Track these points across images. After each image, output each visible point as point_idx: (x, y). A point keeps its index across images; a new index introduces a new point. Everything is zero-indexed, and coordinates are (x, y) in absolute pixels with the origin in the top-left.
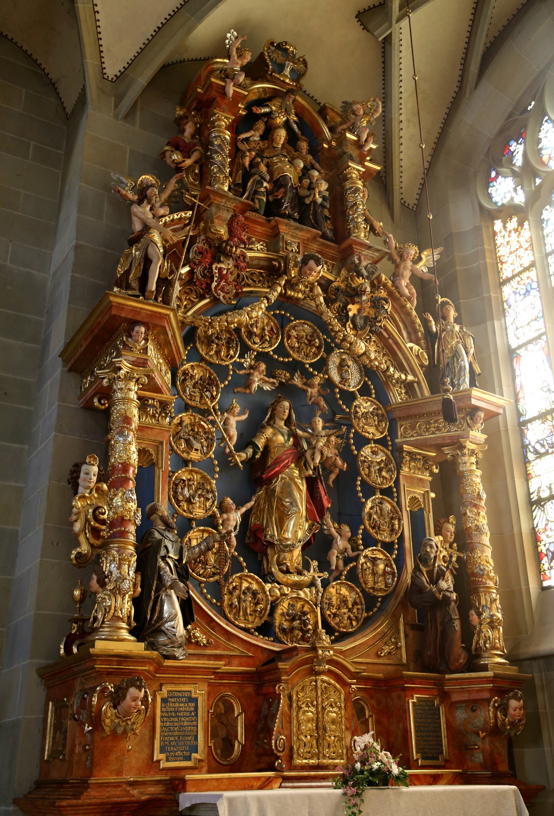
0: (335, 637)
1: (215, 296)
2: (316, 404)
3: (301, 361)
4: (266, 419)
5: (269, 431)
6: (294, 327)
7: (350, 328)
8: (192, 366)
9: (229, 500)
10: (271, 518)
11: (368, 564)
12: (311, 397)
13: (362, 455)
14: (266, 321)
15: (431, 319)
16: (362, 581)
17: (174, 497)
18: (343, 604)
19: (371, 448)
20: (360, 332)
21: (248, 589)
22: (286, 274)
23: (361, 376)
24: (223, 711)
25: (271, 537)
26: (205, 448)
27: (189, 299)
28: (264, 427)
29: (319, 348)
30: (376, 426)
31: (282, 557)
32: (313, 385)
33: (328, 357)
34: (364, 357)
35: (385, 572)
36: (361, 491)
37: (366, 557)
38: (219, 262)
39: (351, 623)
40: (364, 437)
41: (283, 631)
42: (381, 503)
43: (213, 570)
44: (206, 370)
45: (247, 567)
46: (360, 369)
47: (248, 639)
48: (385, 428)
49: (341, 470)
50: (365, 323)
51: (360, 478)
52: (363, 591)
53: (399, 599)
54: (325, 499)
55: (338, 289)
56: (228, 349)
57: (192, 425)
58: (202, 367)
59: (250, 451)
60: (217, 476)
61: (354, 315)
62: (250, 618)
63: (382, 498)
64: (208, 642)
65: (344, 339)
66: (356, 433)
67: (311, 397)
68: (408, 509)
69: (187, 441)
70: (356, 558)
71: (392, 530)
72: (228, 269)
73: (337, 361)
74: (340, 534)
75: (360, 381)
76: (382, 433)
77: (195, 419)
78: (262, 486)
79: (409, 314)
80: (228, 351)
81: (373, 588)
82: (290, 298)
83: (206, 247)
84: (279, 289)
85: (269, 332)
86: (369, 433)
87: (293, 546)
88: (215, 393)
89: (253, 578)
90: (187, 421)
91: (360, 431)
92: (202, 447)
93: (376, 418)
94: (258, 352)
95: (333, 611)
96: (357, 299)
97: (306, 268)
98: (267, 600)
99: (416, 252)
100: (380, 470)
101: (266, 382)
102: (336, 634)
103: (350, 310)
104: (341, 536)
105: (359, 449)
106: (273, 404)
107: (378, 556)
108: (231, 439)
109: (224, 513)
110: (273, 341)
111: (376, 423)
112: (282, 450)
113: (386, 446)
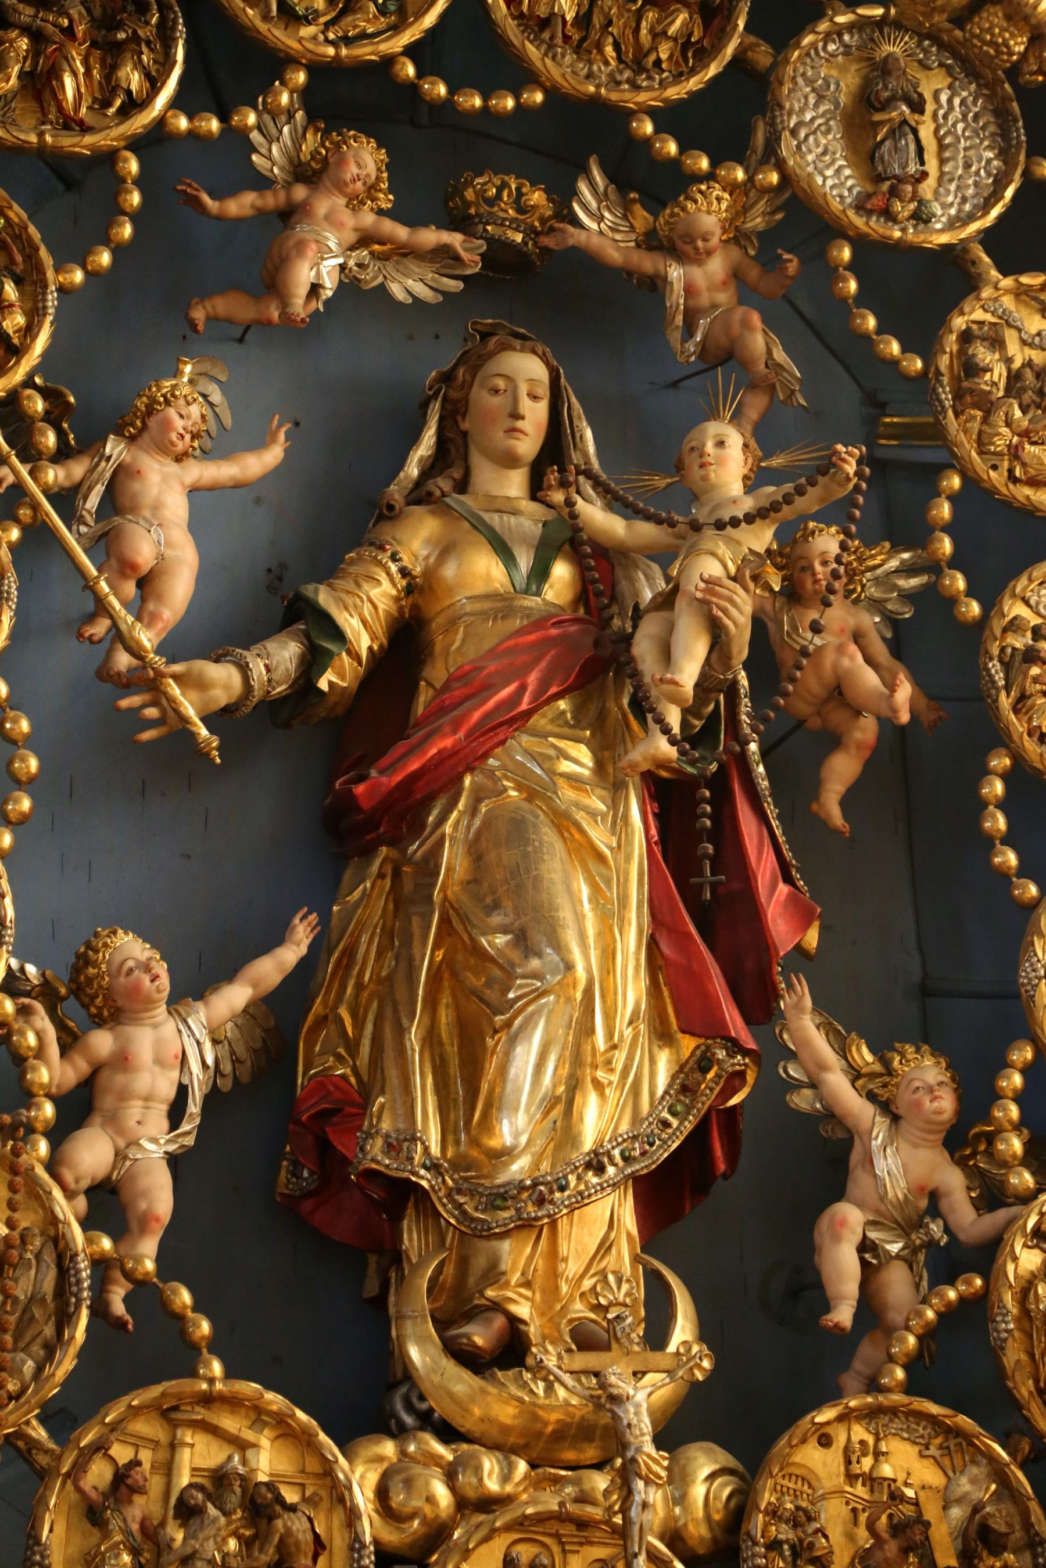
3: (595, 101)
4: (413, 470)
10: (401, 1032)
12: (691, 317)
13: (1014, 625)
23: (1005, 154)
25: (391, 1147)
28: (388, 514)
31: (479, 1263)
32: (690, 238)
33: (779, 62)
36: (1009, 840)
45: (216, 1346)
46: (1001, 114)
49: (887, 724)
51: (1001, 762)
60: (26, 804)
67: (691, 317)
74: (886, 1107)
78: (368, 852)
80: (110, 71)
89: (259, 1415)
91: (997, 478)
94: (317, 69)
98: (356, 1544)
101: (405, 252)
104: (896, 1119)
106: (447, 378)
109: (99, 1022)
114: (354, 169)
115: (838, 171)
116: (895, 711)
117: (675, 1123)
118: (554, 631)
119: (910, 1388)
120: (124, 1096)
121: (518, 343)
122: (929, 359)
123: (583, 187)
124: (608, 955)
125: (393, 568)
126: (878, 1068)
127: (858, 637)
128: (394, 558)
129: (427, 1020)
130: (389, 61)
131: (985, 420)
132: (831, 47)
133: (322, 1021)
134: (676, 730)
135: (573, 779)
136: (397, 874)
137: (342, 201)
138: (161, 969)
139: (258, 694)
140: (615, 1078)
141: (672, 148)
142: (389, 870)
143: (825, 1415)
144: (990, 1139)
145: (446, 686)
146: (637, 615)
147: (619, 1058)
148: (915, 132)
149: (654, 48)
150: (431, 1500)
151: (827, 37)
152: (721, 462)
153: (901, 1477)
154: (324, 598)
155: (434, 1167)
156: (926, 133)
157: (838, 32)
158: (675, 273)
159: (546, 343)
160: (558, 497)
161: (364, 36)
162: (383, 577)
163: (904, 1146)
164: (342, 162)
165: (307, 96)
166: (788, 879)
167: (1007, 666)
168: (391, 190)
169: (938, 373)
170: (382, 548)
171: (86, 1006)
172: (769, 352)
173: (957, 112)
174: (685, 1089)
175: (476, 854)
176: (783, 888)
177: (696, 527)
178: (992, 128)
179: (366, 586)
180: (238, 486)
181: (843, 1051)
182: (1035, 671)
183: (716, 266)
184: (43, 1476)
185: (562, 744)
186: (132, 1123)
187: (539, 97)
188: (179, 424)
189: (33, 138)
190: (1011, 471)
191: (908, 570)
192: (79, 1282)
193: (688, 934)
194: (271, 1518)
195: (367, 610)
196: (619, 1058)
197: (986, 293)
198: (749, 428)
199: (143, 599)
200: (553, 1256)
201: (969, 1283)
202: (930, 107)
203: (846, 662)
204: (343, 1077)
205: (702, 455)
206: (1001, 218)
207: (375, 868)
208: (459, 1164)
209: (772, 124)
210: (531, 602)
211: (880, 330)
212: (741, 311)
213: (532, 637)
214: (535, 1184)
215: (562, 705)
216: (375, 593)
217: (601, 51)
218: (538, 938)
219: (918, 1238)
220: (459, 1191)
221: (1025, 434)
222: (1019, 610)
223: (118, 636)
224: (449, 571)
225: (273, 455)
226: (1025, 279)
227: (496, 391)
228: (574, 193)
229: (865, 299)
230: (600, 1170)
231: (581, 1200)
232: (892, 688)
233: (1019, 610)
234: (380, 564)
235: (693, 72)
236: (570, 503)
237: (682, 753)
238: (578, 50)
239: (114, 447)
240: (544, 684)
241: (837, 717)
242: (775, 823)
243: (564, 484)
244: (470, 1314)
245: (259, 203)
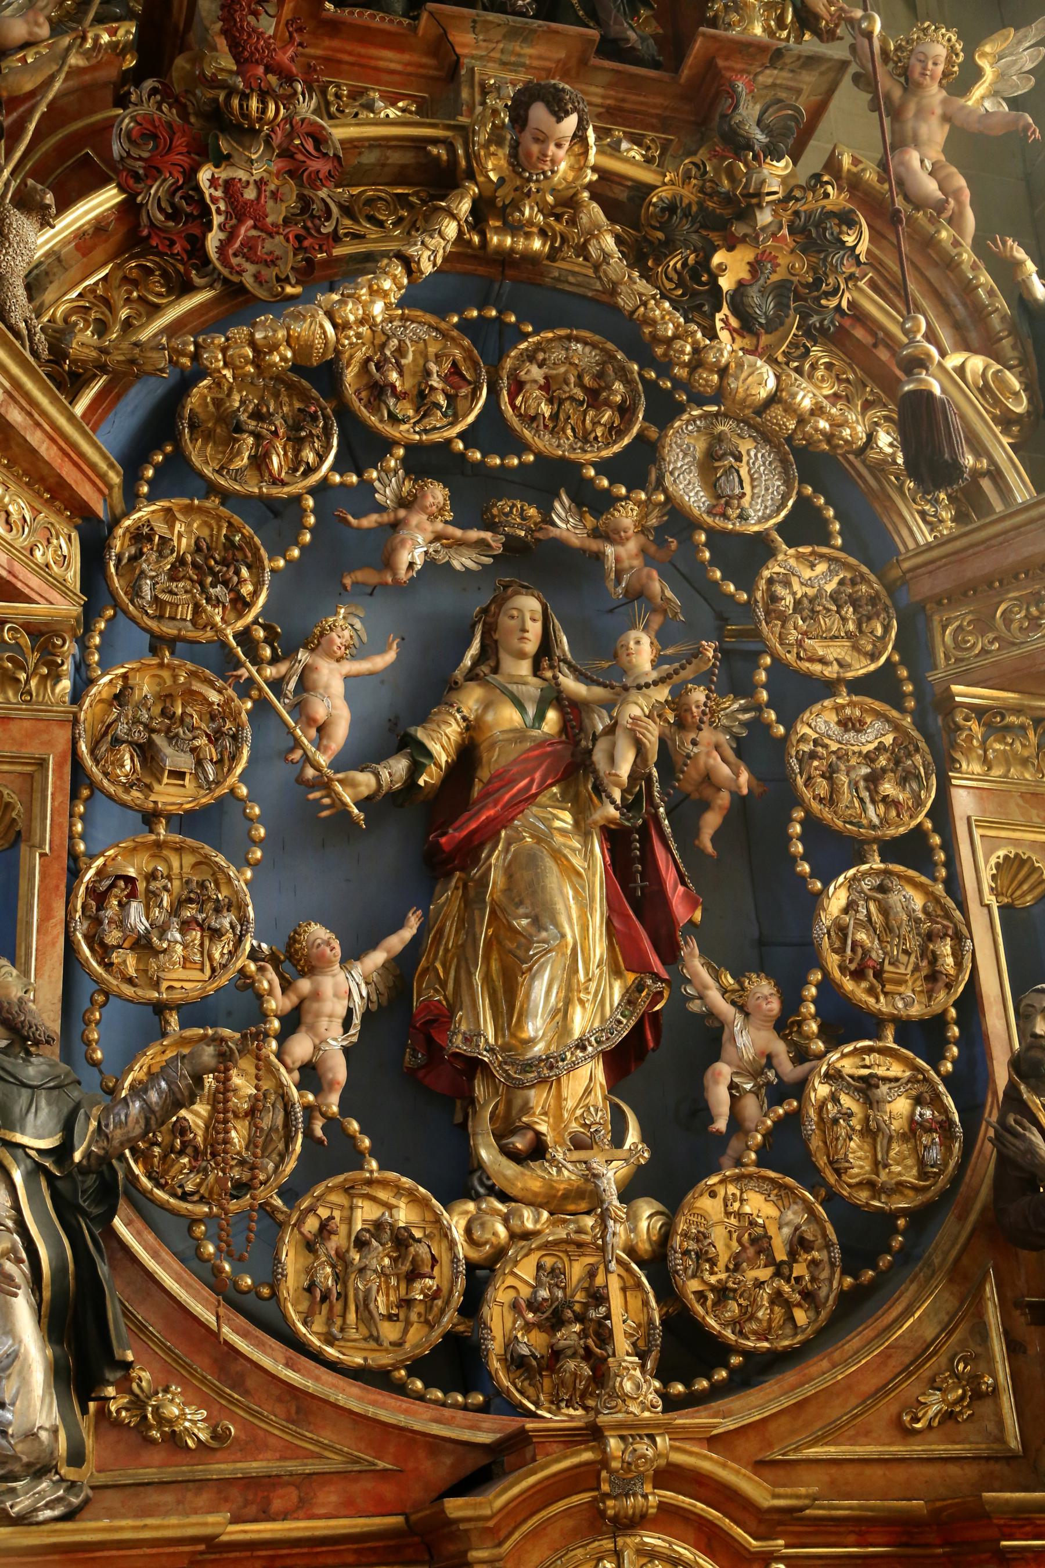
0: (732, 1371)
1: (226, 281)
2: (637, 595)
3: (562, 459)
4: (468, 662)
5: (471, 700)
6: (530, 356)
7: (732, 331)
8: (168, 511)
9: (318, 932)
10: (470, 975)
11: (846, 1101)
13: (803, 739)
14: (432, 350)
15: (1020, 254)
16: (822, 1161)
17: (89, 939)
18: (751, 1251)
19: (838, 709)
20: (765, 339)
21: (378, 1225)
22: (471, 176)
23: (787, 483)
25: (467, 1040)
26: (210, 769)
27: (141, 299)
28: (455, 687)
29: (625, 411)
30: (849, 635)
31: (518, 1103)
32: (617, 531)
34: (776, 412)
35: (914, 1129)
36: (805, 857)
37: (833, 1076)
38: (220, 160)
39: (791, 1319)
40: (808, 676)
41: (516, 1363)
42: (882, 889)
43: (236, 1174)
44: (219, 518)
45: (373, 1152)
46: (784, 462)
47: (371, 1411)
48: (883, 638)
49: (736, 796)
50: (782, 306)
51: (798, 814)
52: (831, 1199)
53: (973, 1217)
54: (676, 895)
55: (671, 208)
56: (297, 443)
57: (166, 698)
58: (200, 510)
59: (400, 765)
60: (259, 854)
61: (741, 284)
62: (389, 1332)
63: (887, 873)
64: (215, 1436)
65: (697, 362)
66: (779, 666)
68: (990, 899)
69: (147, 753)
70: (799, 1088)
71: (933, 977)
72: (260, 184)
73: (700, 446)
74: (742, 1008)
75: (785, 498)
76: (873, 657)
77: (175, 677)
78: (449, 875)
79: (950, 264)
80: (297, 452)
81: (870, 1185)
82: (505, 260)
83: (169, 114)
84: (451, 229)
85: (445, 379)
86: (822, 661)
87: (550, 1062)
88: (247, 589)
89: (399, 1190)
90: (145, 687)
91: (791, 658)
92: (199, 763)
93: (849, 611)
94: (410, 447)
95: (713, 1280)
96: (739, 229)
97: (527, 137)
98: (454, 1260)
99: (952, 49)
100: (873, 780)
101: (460, 544)
102: (735, 1360)
103: (722, 268)
104: (747, 1015)
105: (789, 721)
106: (485, 611)
107: (881, 1072)
108: (323, 729)
109: (303, 974)
110: (462, 405)
111: (851, 626)
112: (514, 751)
113: (896, 701)
114: (431, 500)
115: (697, 493)
116: (739, 788)
117: (625, 1021)
118: (549, 749)
119: (759, 1164)
120: (318, 1015)
121: (524, 591)
122: (750, 593)
123: (557, 505)
124: (585, 928)
125: (458, 716)
126: (736, 987)
127: (717, 747)
128: (459, 711)
129: (484, 968)
130: (449, 441)
131: (783, 626)
132: (690, 428)
133: (426, 970)
134: (619, 802)
135: (562, 831)
136: (465, 886)
137: (425, 517)
138: (336, 944)
139: (385, 788)
140: (590, 997)
141: (605, 483)
142: (461, 885)
143: (713, 1180)
144: (800, 1024)
145: (489, 782)
146: (595, 738)
147: (593, 986)
148: (738, 472)
149: (594, 430)
150: (495, 1234)
151: (688, 423)
152: (638, 653)
153: (755, 1213)
154: (420, 734)
155: (491, 1050)
156: (744, 472)
157: (694, 419)
158: (609, 550)
159: (540, 590)
160: (549, 674)
161: (435, 428)
162: (453, 721)
163: (752, 1029)
164: (424, 496)
165: (404, 461)
166: (684, 883)
167: (800, 761)
168: (451, 510)
169: (756, 601)
170: (452, 706)
171: (295, 966)
172: (663, 592)
173: (760, 461)
174: (629, 1002)
175: (509, 873)
176: (681, 889)
177: (626, 689)
178: (779, 469)
179: (443, 727)
180: (371, 674)
181: (717, 978)
182: (816, 763)
183: (632, 546)
184: (281, 1225)
185: (555, 811)
186: (323, 1030)
187: (531, 458)
188: (338, 641)
189: (256, 490)
190: (798, 654)
191: (744, 710)
192: (296, 1119)
193: (629, 916)
194: (407, 1246)
195: (444, 740)
196: (593, 986)
197: (780, 557)
198: (653, 634)
199: (320, 738)
200: (559, 1097)
201: (790, 1104)
202: (745, 458)
203: (711, 761)
204: (439, 1001)
205: (628, 648)
206: (786, 517)
207: (453, 884)
208: (505, 1048)
209: (660, 469)
210: (536, 733)
211: (723, 578)
212: (646, 570)
213: (537, 752)
214: (548, 1058)
215: (555, 789)
216: (448, 731)
217: (564, 433)
218: (545, 920)
219: (761, 1080)
220: (506, 1063)
221: (805, 634)
222: (806, 730)
223: (307, 759)
224: (489, 717)
225: (390, 656)
226: (801, 550)
227: (513, 617)
228: (552, 508)
229: (714, 562)
230: (584, 1049)
231: (574, 1066)
232: (737, 775)
233: (806, 730)
234: (451, 714)
235: (615, 442)
236: (555, 678)
237: (622, 814)
238: (552, 432)
239: (303, 655)
240: (543, 780)
241: (708, 792)
242: (675, 852)
243: (552, 667)
244: (514, 1132)
245: (380, 520)
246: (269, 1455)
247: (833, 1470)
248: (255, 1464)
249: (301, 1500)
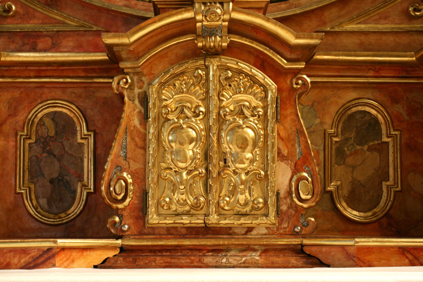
24: (52, 133)
246: (36, 21)
247: (363, 38)
248: (28, 25)
249: (53, 44)
